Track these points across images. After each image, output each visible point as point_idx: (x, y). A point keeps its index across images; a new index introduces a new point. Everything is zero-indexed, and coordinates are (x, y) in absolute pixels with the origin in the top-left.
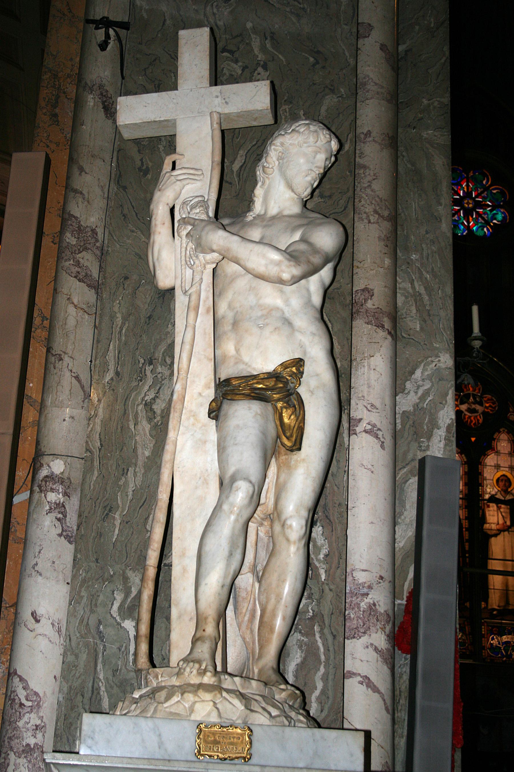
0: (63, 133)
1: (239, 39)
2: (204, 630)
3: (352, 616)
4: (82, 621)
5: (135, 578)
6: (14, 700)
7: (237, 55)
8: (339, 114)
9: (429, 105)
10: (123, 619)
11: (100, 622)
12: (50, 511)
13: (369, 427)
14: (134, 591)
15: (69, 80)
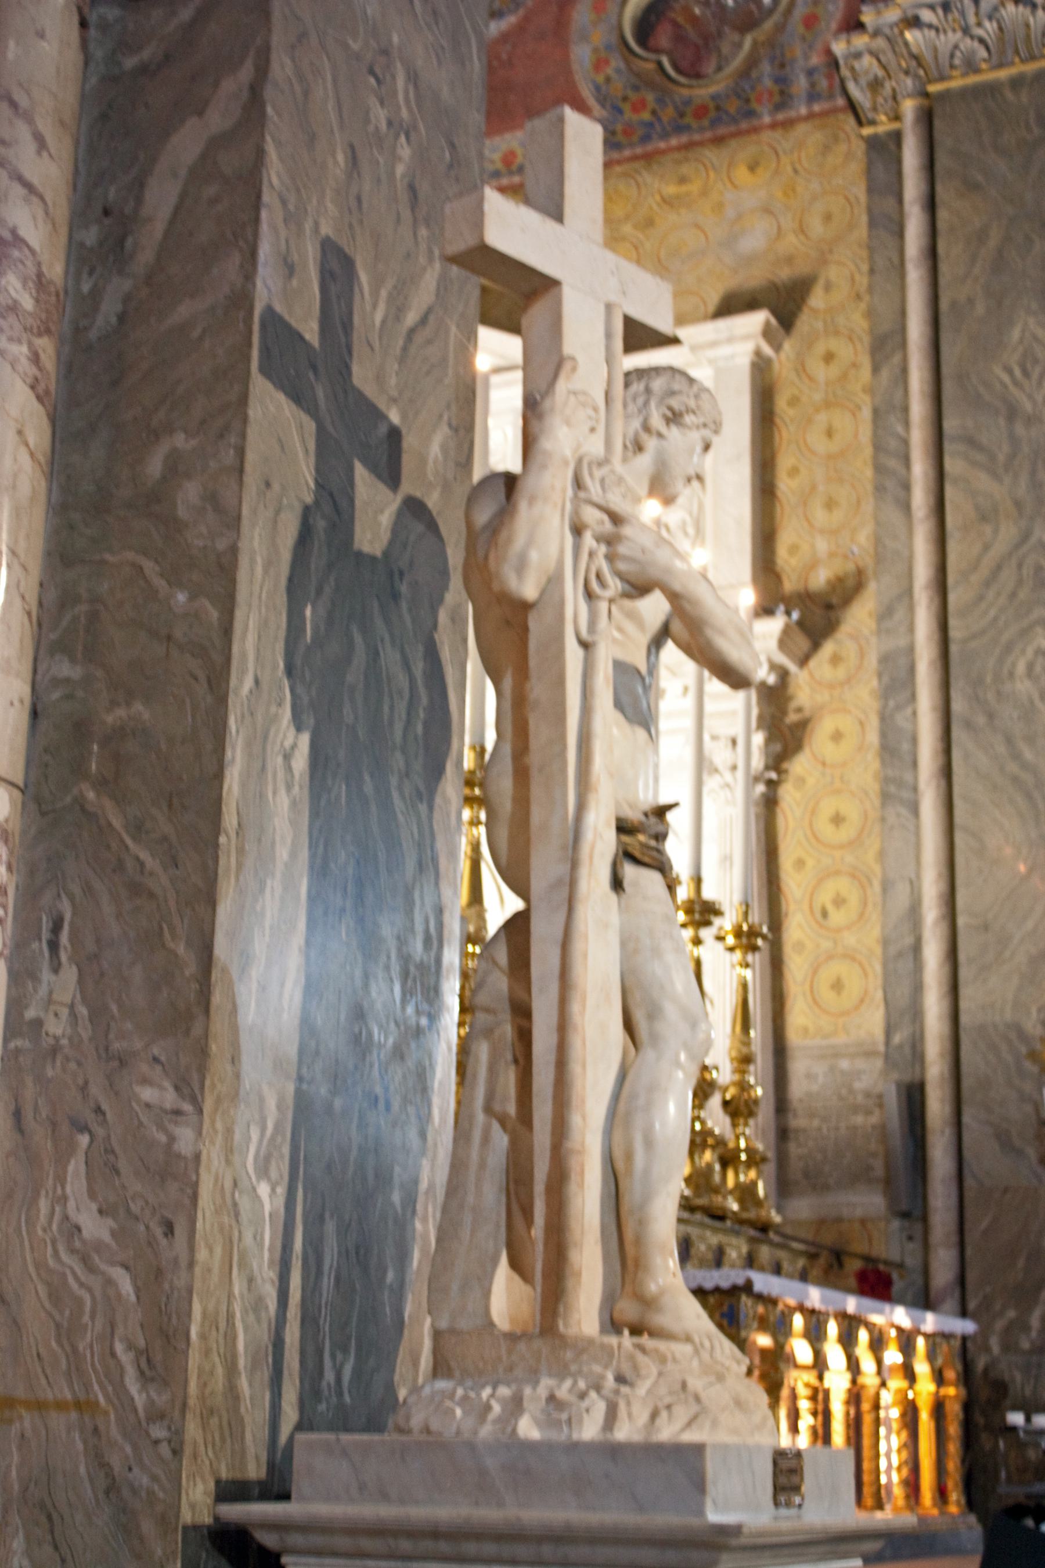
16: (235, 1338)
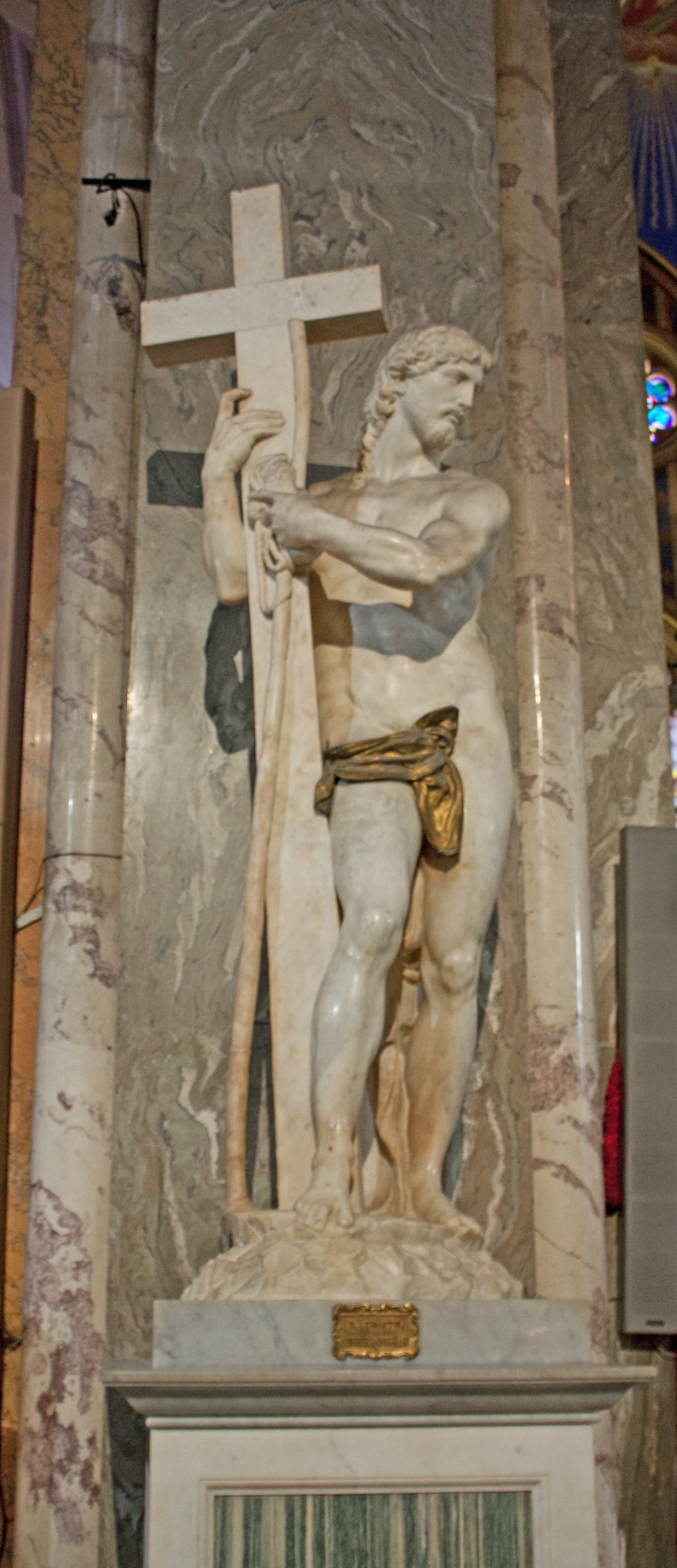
0: (56, 355)
1: (319, 197)
2: (330, 1149)
3: (538, 1076)
4: (136, 1116)
5: (212, 1048)
6: (41, 1226)
7: (318, 222)
8: (479, 308)
9: (609, 285)
10: (199, 1109)
11: (163, 1117)
12: (75, 940)
13: (548, 788)
14: (212, 1067)
15: (60, 273)
16: (171, 1234)
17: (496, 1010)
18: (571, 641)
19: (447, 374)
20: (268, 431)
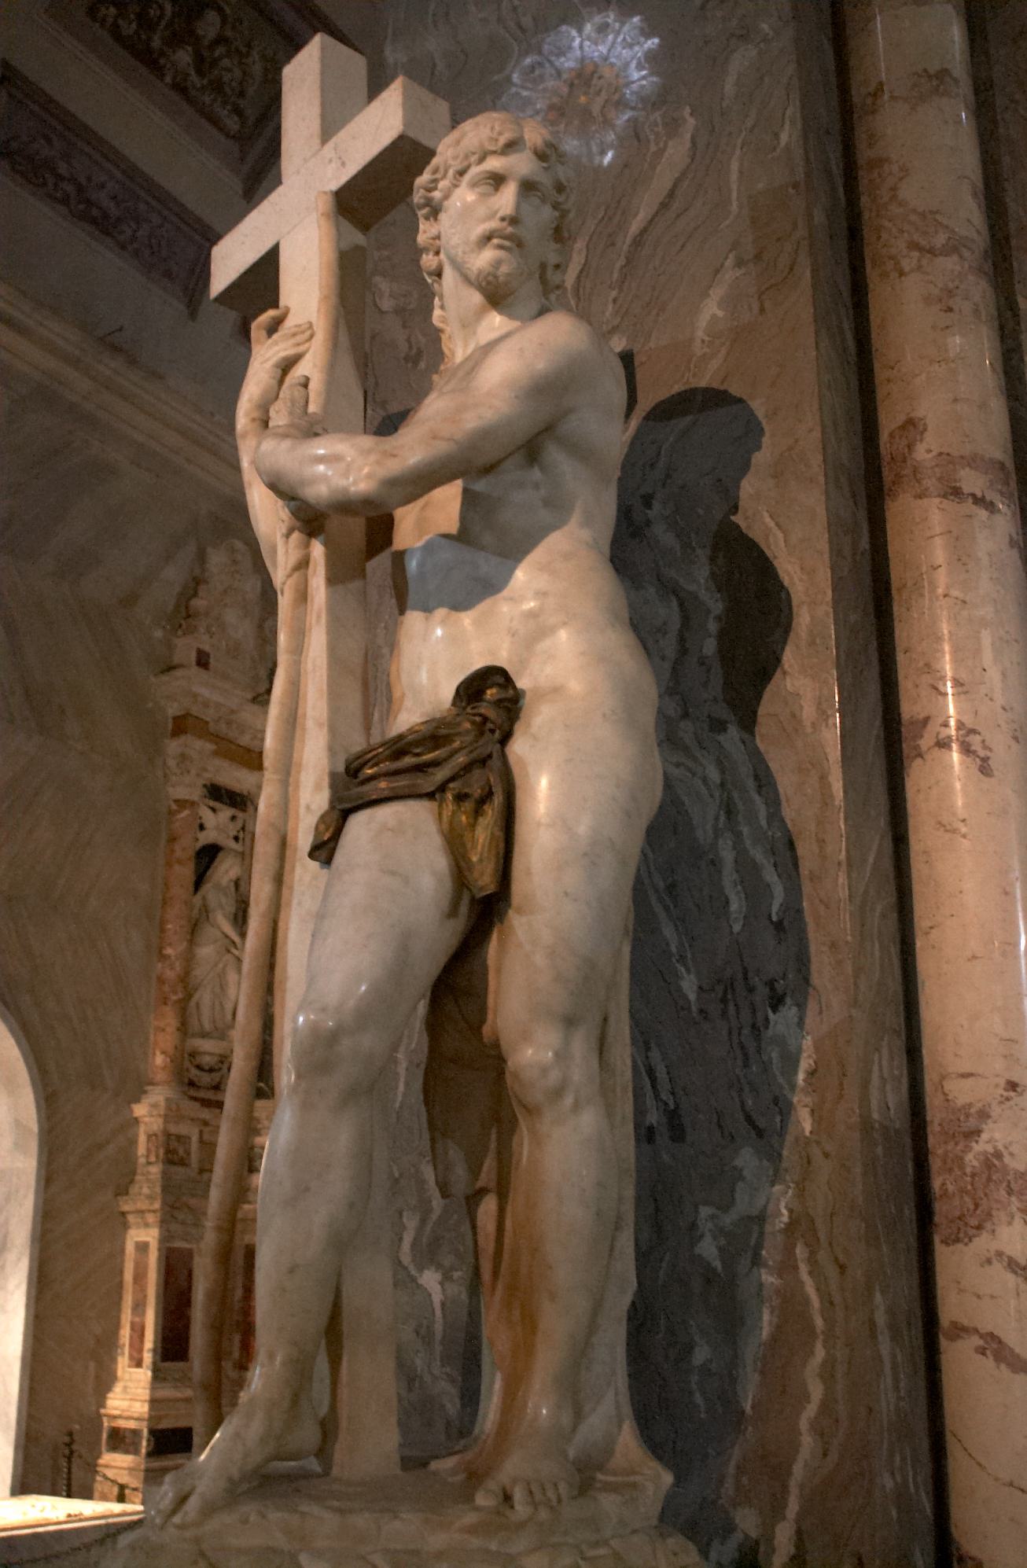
3: (951, 1188)
8: (762, 78)
10: (421, 1269)
17: (808, 1100)
18: (979, 501)
19: (473, 185)
20: (291, 352)
